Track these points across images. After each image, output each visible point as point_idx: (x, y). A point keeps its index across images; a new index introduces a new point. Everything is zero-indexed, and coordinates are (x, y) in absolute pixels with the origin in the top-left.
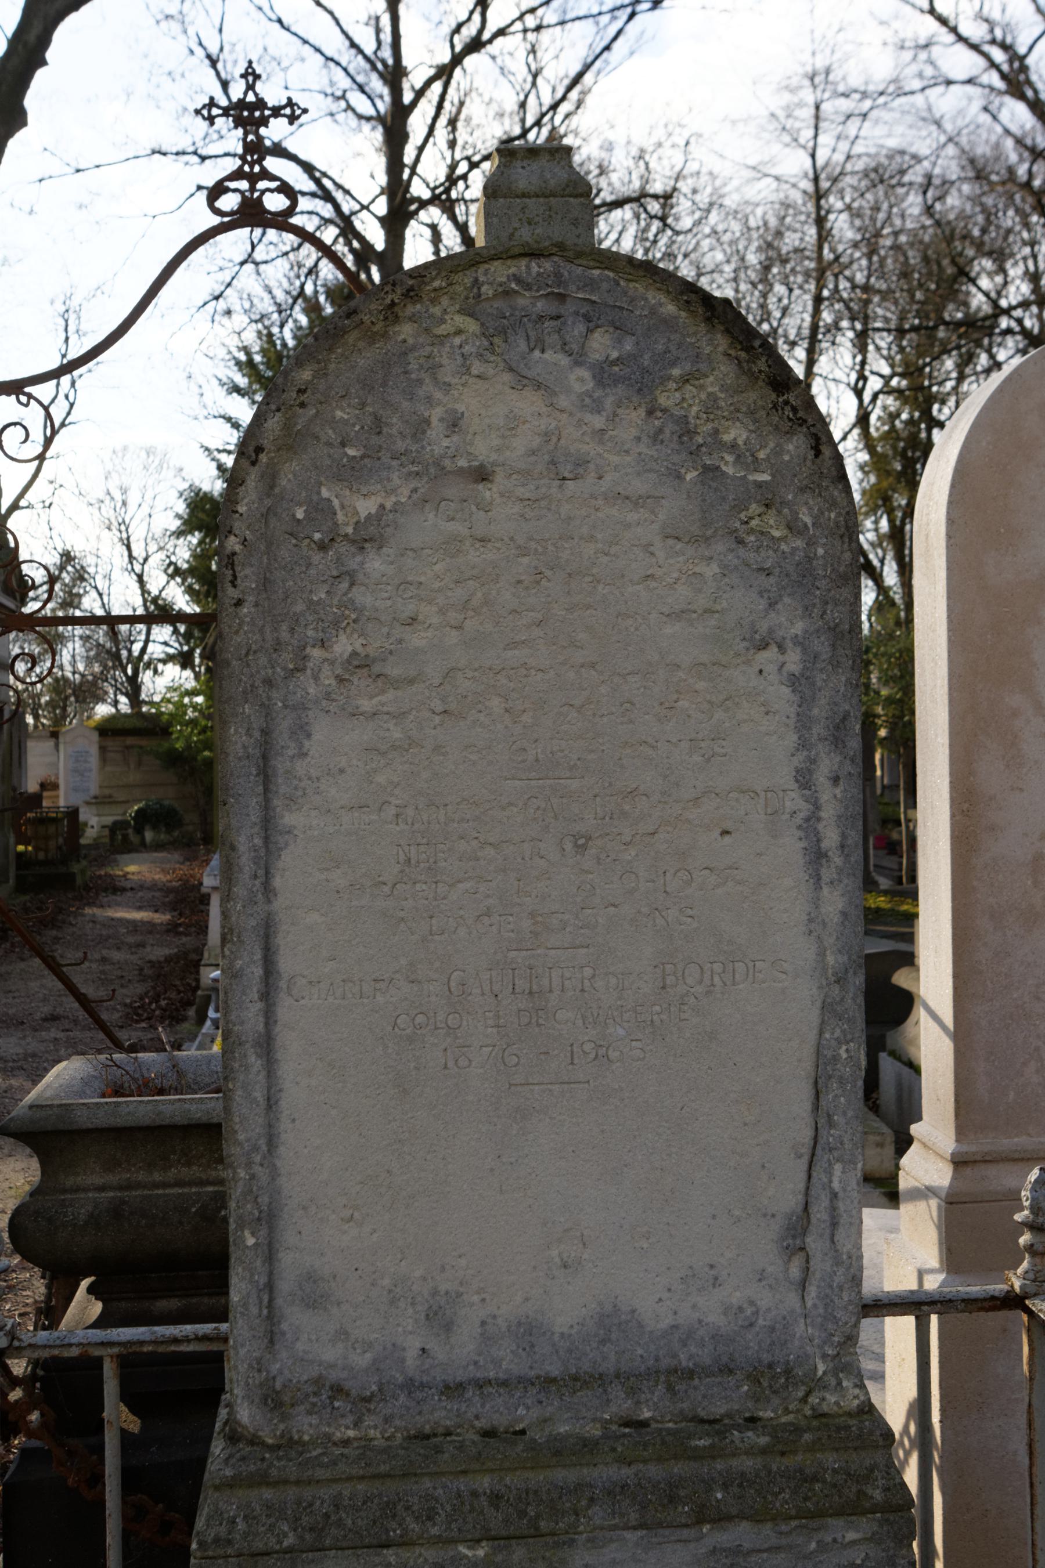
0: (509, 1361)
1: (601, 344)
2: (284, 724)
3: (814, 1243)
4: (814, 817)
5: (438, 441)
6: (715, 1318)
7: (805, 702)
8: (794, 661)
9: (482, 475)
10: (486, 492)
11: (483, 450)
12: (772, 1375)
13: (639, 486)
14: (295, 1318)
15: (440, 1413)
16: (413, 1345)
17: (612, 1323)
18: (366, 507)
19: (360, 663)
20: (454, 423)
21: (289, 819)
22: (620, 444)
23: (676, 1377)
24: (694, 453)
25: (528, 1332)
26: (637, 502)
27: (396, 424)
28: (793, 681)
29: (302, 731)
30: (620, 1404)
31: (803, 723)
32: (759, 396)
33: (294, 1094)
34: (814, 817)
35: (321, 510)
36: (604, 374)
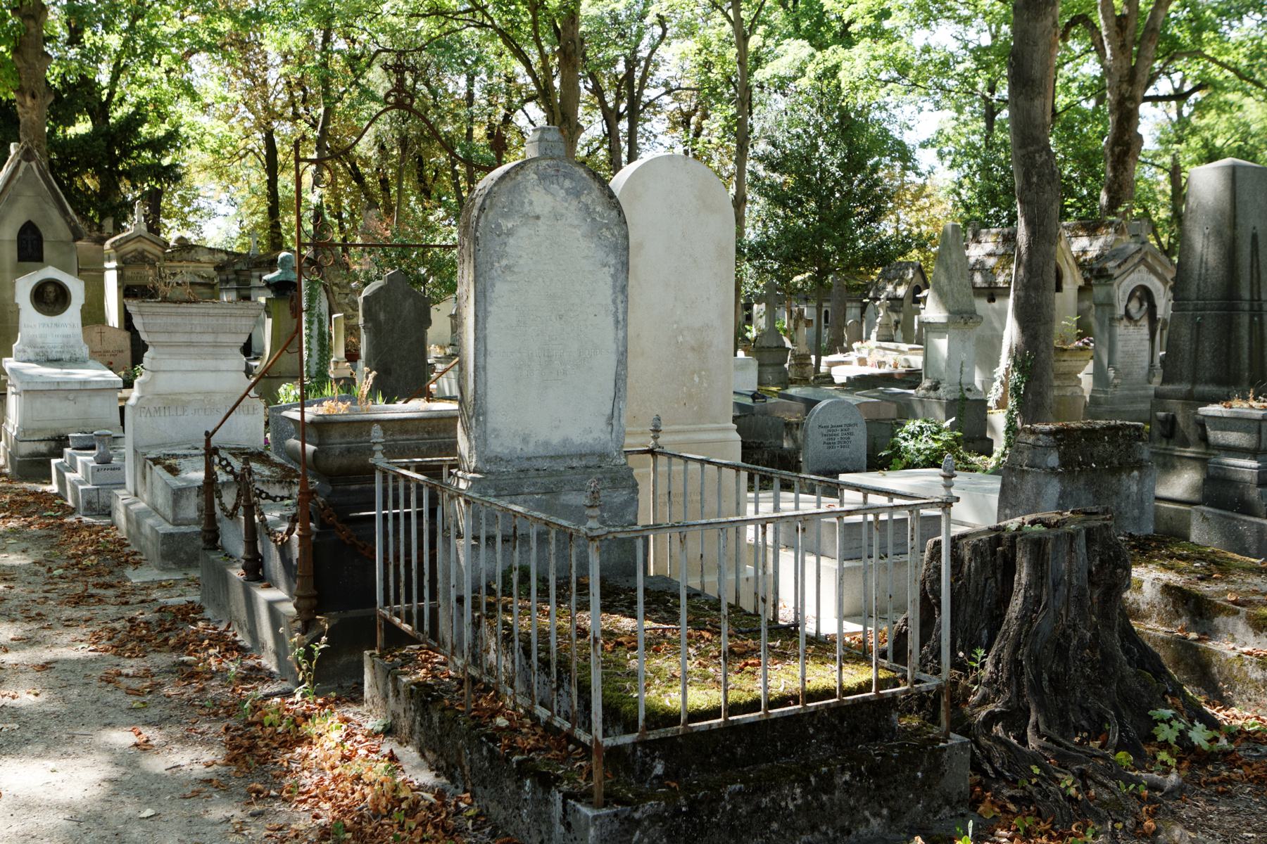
0: (542, 452)
1: (567, 183)
2: (488, 285)
3: (614, 422)
4: (616, 312)
5: (527, 208)
6: (591, 441)
7: (615, 281)
9: (538, 217)
10: (540, 223)
11: (538, 211)
12: (603, 456)
13: (576, 222)
15: (526, 465)
16: (519, 447)
18: (510, 225)
19: (508, 267)
20: (531, 203)
21: (490, 309)
22: (571, 211)
23: (581, 456)
24: (589, 214)
25: (546, 444)
26: (575, 227)
27: (516, 202)
28: (612, 276)
29: (493, 285)
30: (569, 462)
31: (614, 287)
34: (616, 312)
35: (499, 226)
36: (568, 192)
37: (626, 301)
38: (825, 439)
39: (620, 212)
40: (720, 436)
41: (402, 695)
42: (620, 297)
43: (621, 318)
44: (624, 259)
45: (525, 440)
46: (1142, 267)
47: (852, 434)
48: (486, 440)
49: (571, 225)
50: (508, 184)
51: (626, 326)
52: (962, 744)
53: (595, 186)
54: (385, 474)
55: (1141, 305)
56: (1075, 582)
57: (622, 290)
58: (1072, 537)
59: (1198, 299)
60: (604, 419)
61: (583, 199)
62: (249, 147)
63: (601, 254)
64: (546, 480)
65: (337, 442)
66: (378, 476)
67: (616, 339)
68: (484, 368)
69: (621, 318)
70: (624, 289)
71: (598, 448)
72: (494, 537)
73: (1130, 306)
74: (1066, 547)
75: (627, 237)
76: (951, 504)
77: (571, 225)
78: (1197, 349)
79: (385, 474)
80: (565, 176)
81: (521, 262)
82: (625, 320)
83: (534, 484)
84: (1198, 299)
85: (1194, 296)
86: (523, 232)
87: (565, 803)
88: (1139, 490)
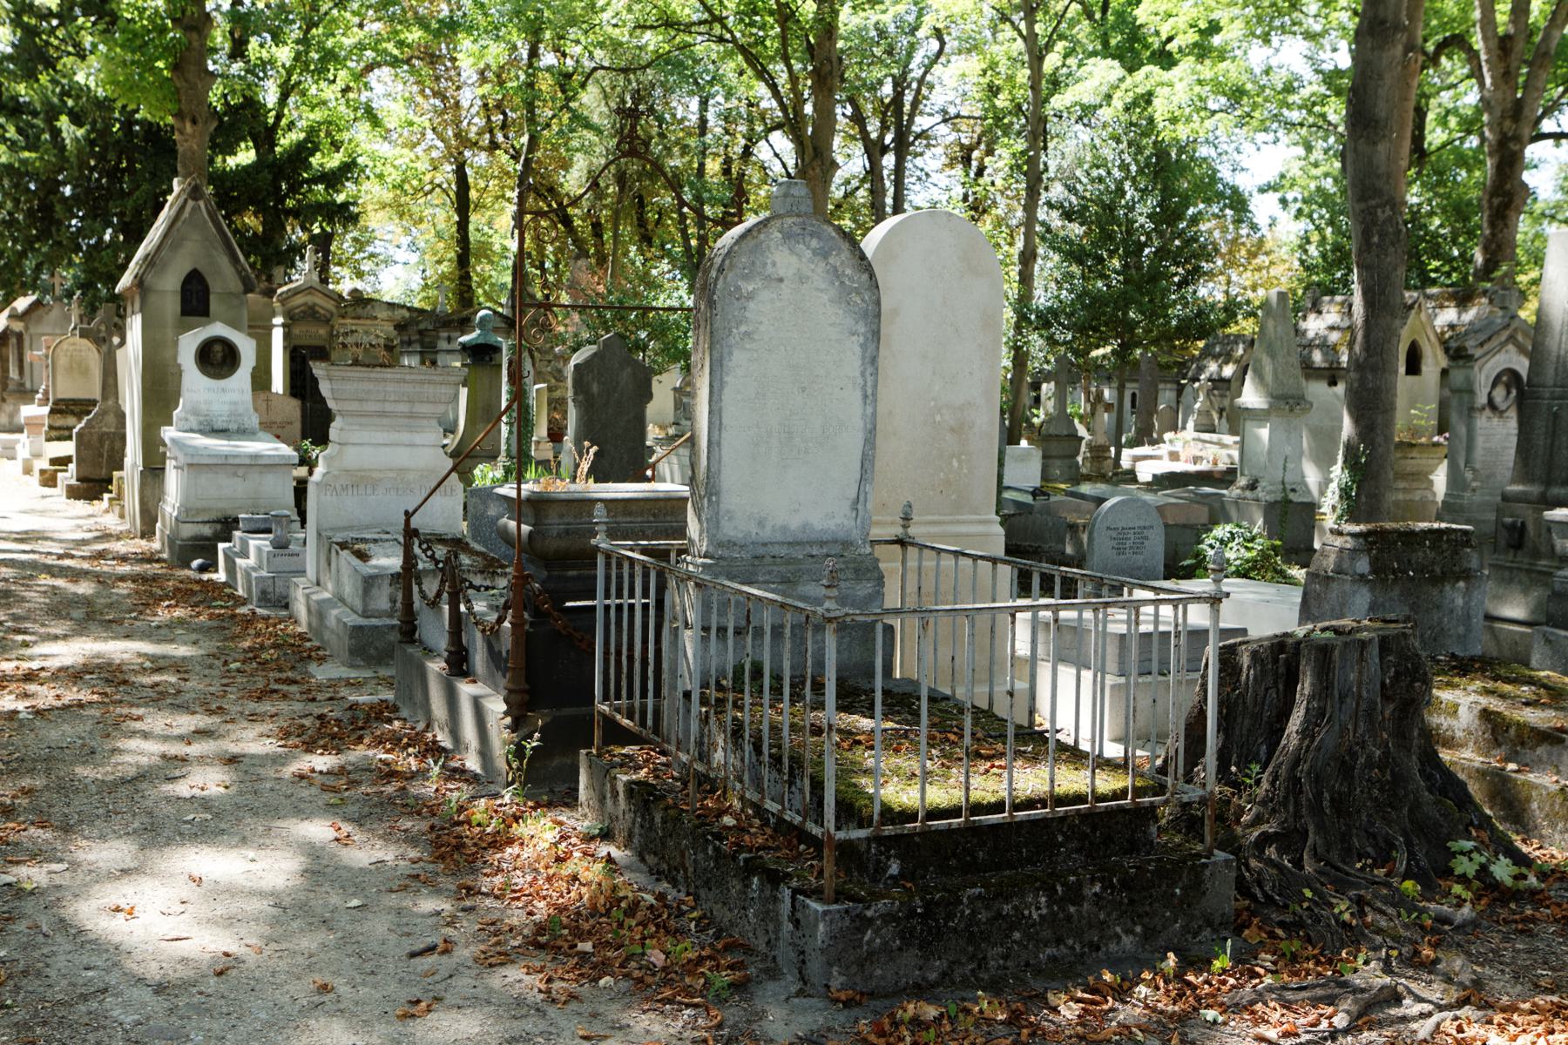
0: (779, 537)
1: (814, 243)
2: (726, 350)
3: (860, 507)
5: (769, 269)
8: (861, 339)
9: (781, 280)
11: (782, 273)
12: (847, 544)
13: (823, 286)
14: (724, 523)
15: (761, 551)
17: (805, 526)
18: (750, 288)
19: (747, 334)
20: (774, 264)
21: (726, 379)
23: (822, 544)
25: (784, 529)
29: (731, 353)
30: (808, 550)
31: (863, 358)
32: (856, 261)
33: (725, 459)
35: (738, 288)
36: (814, 252)
37: (875, 374)
38: (1114, 543)
39: (872, 275)
40: (981, 529)
41: (621, 795)
42: (870, 370)
43: (869, 392)
44: (874, 327)
45: (761, 524)
46: (1511, 347)
47: (1146, 538)
48: (718, 522)
49: (817, 289)
50: (750, 242)
51: (875, 401)
52: (1226, 861)
53: (845, 246)
54: (608, 556)
55: (1509, 393)
56: (1365, 694)
57: (872, 362)
58: (1363, 644)
59: (1555, 386)
60: (849, 503)
61: (831, 260)
62: (437, 181)
63: (849, 321)
64: (782, 569)
65: (555, 523)
66: (600, 560)
67: (864, 415)
68: (719, 444)
69: (869, 392)
70: (874, 360)
71: (841, 535)
72: (725, 630)
73: (1495, 393)
74: (1356, 655)
75: (878, 303)
76: (1220, 600)
77: (817, 289)
78: (1552, 445)
79: (608, 556)
80: (812, 235)
81: (762, 328)
82: (874, 394)
83: (770, 573)
84: (1555, 386)
85: (1551, 382)
86: (765, 295)
87: (793, 899)
88: (1466, 603)
